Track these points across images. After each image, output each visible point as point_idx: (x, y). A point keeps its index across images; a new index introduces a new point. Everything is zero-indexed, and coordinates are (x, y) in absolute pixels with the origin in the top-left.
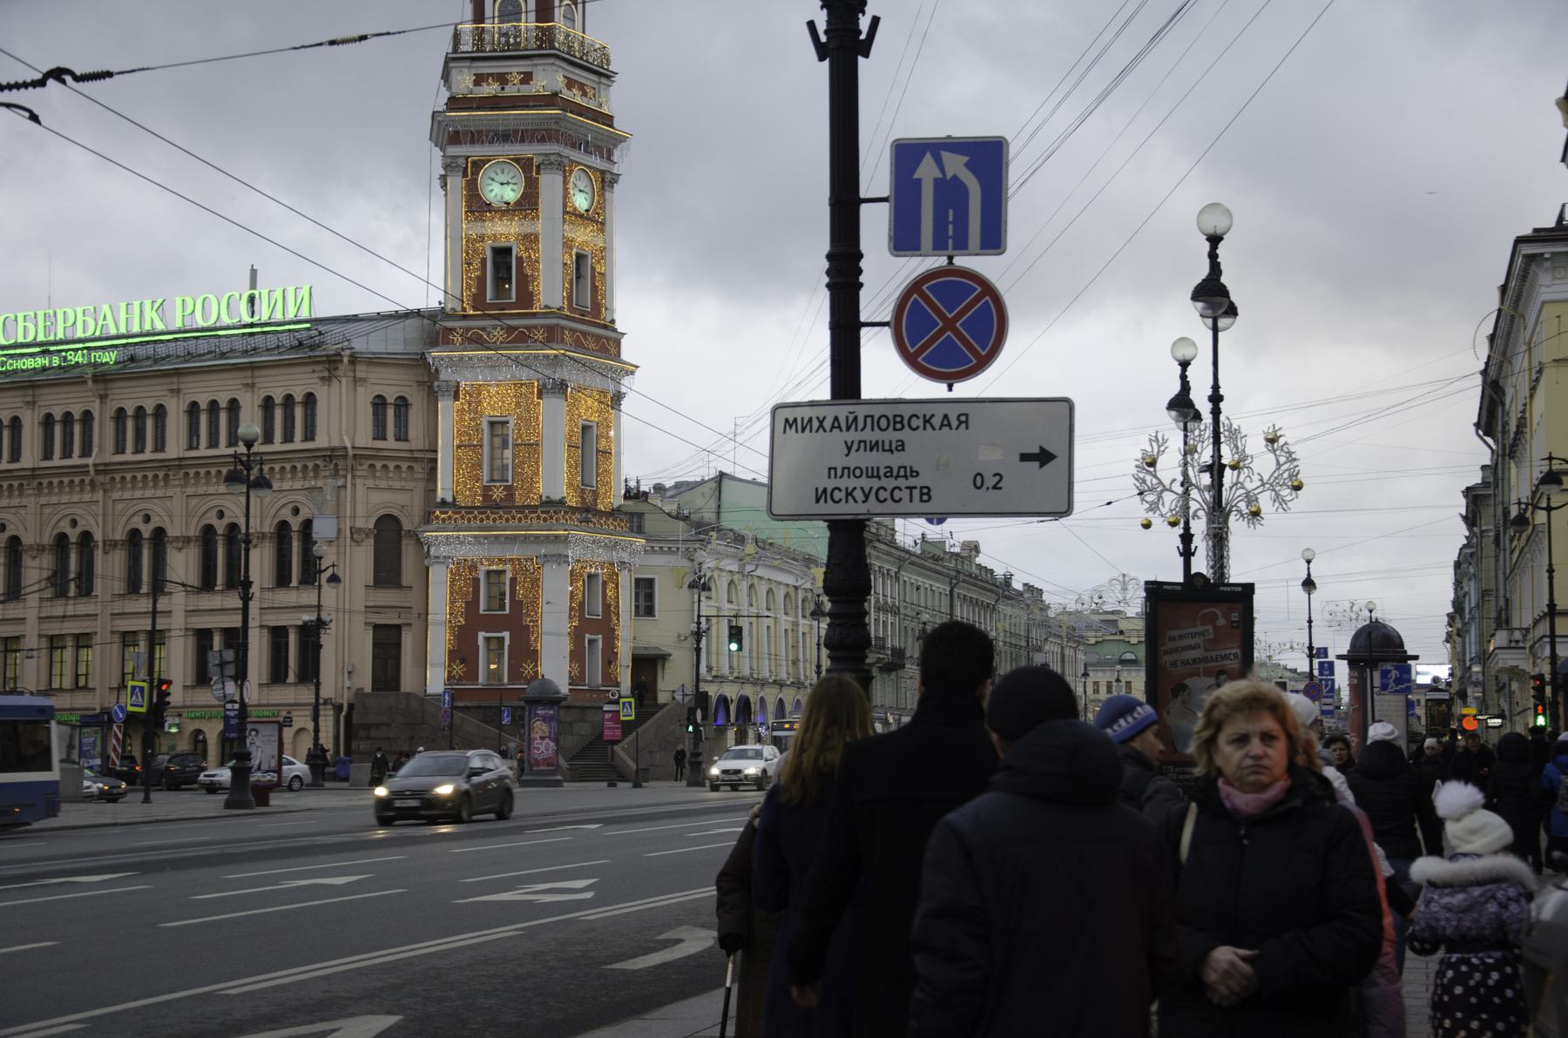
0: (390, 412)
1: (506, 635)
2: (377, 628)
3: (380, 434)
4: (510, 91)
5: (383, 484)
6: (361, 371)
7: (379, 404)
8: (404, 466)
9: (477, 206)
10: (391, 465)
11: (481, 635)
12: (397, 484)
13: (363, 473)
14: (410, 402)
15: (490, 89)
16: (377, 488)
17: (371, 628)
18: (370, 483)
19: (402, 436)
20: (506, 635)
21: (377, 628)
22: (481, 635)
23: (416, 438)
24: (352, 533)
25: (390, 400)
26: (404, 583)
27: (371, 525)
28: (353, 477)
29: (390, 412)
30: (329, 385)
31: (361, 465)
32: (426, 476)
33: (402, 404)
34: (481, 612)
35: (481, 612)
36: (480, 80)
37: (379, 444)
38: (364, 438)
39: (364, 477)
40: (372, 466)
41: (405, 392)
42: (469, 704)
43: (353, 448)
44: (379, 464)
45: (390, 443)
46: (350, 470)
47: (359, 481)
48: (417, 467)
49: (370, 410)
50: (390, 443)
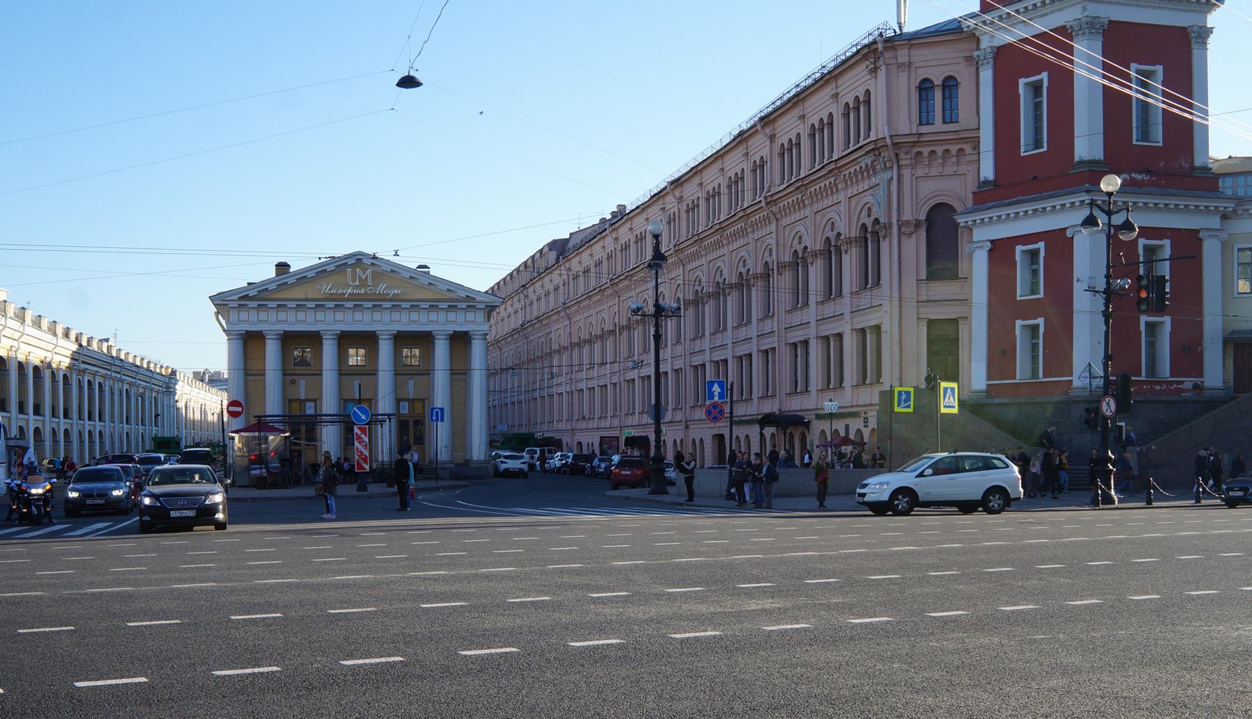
1: (1040, 321)
2: (931, 323)
3: (925, 117)
7: (925, 87)
8: (954, 149)
10: (939, 150)
11: (1019, 323)
13: (908, 162)
14: (959, 81)
16: (927, 176)
17: (926, 323)
18: (920, 172)
19: (950, 116)
20: (1040, 321)
21: (931, 323)
22: (1019, 323)
24: (899, 228)
25: (938, 81)
26: (960, 276)
27: (923, 216)
28: (899, 167)
29: (938, 95)
30: (876, 77)
31: (907, 153)
33: (950, 84)
34: (1018, 298)
35: (1018, 298)
37: (924, 129)
38: (906, 125)
40: (919, 153)
42: (1004, 401)
44: (926, 151)
45: (938, 125)
46: (895, 161)
47: (906, 173)
50: (938, 125)
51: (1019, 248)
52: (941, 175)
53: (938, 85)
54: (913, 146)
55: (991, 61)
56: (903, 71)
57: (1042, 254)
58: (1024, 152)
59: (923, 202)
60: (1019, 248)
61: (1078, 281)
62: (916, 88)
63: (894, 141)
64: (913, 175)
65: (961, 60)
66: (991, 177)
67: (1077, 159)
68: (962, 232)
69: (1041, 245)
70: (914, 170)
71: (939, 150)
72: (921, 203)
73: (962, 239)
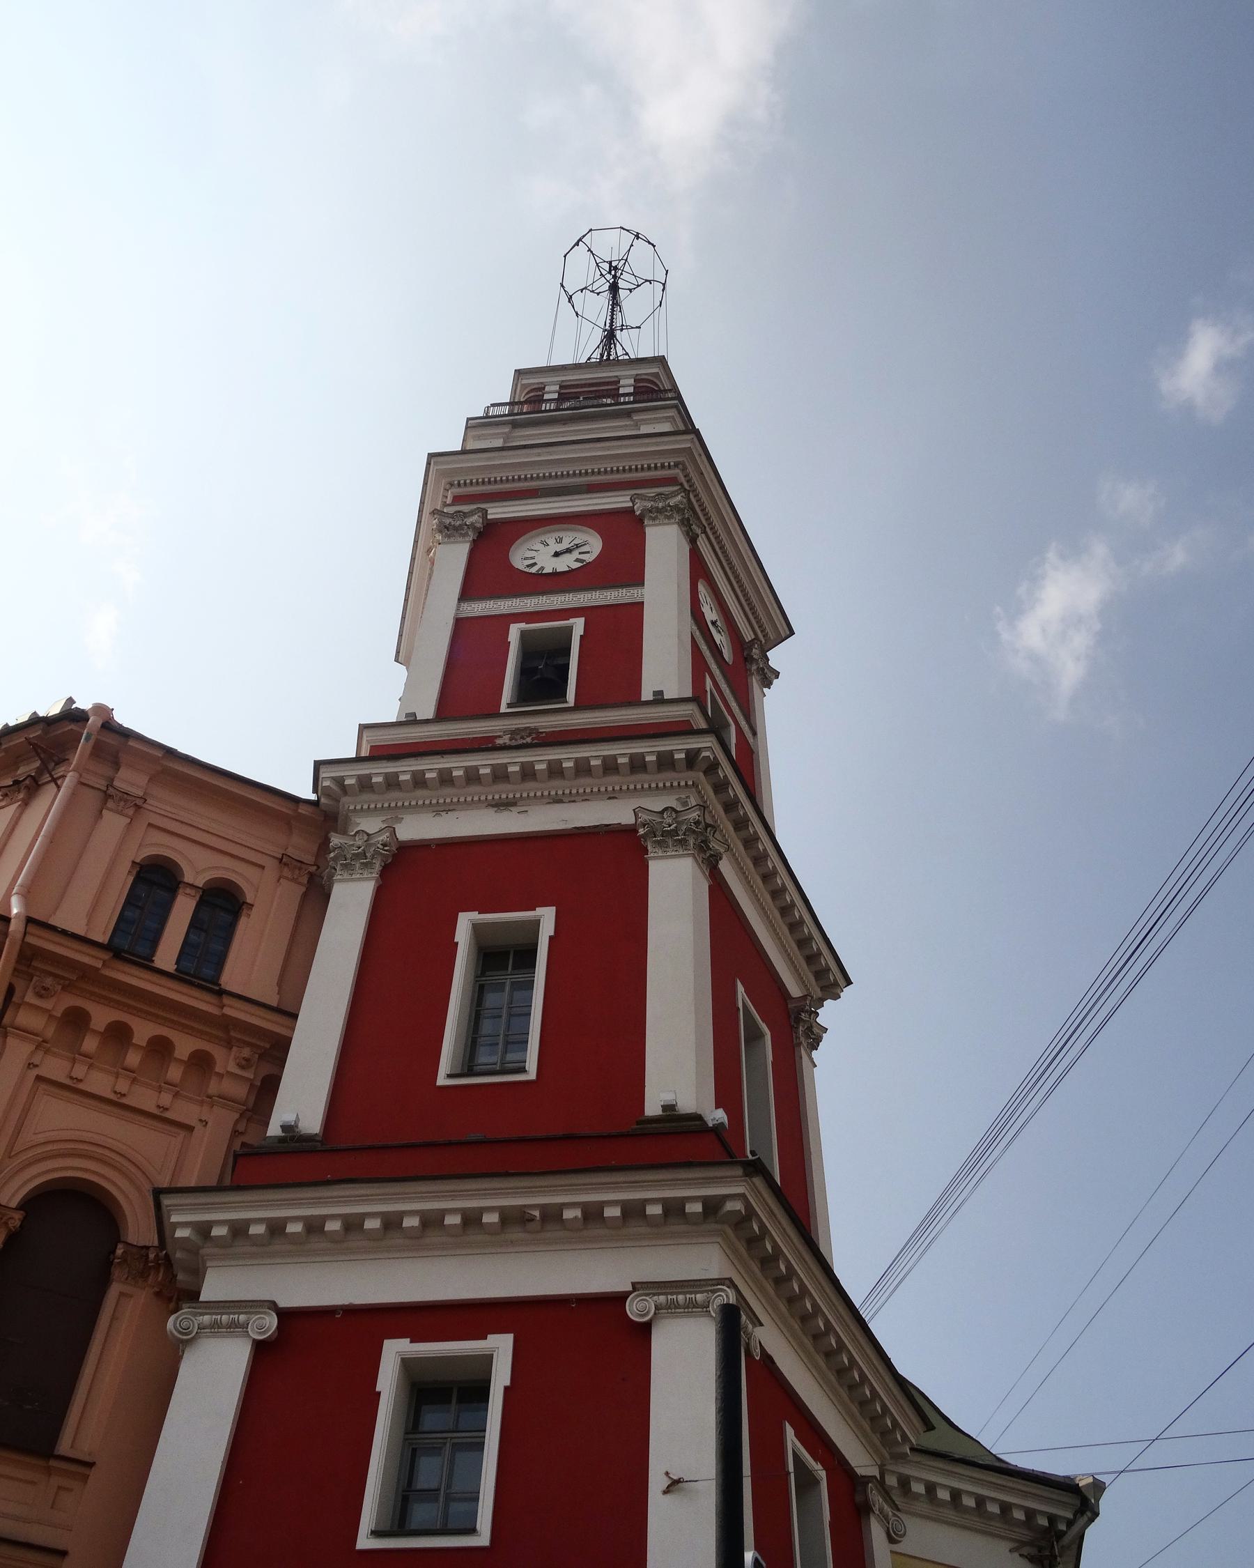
0: (183, 910)
5: (99, 1082)
10: (143, 1031)
12: (145, 1098)
16: (72, 1089)
18: (55, 1068)
26: (64, 1446)
29: (183, 910)
31: (43, 993)
32: (239, 1091)
39: (42, 1045)
40: (76, 1021)
41: (243, 877)
43: (30, 921)
44: (101, 1016)
48: (225, 1060)
49: (123, 881)
51: (394, 1351)
52: (117, 1105)
53: (192, 886)
54: (68, 987)
55: (378, 866)
56: (121, 813)
57: (501, 1377)
58: (450, 1076)
59: (24, 1157)
60: (394, 1351)
61: (674, 1485)
62: (134, 862)
63: (29, 939)
64: (31, 1066)
65: (270, 864)
66: (312, 1123)
67: (652, 1108)
68: (122, 1294)
69: (501, 1347)
70: (40, 1054)
71: (143, 1031)
72: (24, 1157)
73: (114, 1318)
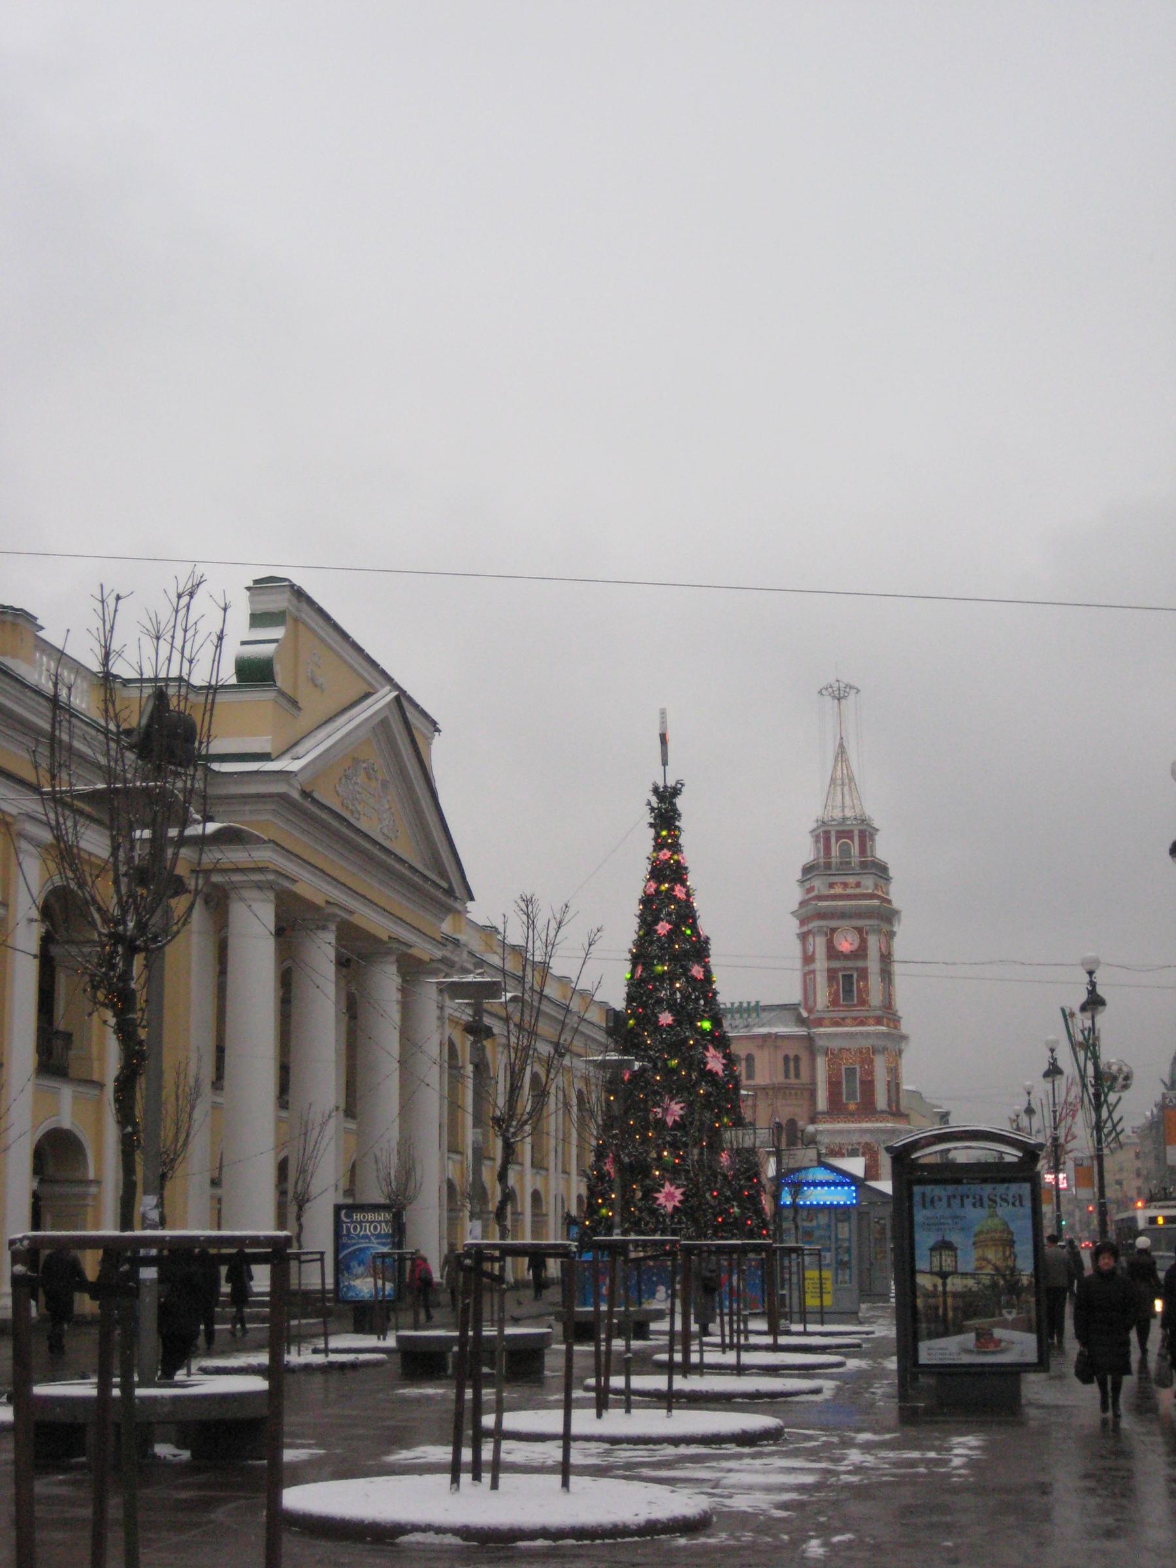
0: (792, 1064)
3: (787, 1076)
4: (849, 891)
6: (779, 1043)
7: (786, 1058)
9: (832, 953)
15: (838, 890)
18: (784, 1102)
19: (797, 1076)
23: (805, 1077)
25: (792, 1056)
29: (792, 1064)
33: (797, 1059)
36: (831, 885)
38: (780, 1079)
50: (793, 1080)
